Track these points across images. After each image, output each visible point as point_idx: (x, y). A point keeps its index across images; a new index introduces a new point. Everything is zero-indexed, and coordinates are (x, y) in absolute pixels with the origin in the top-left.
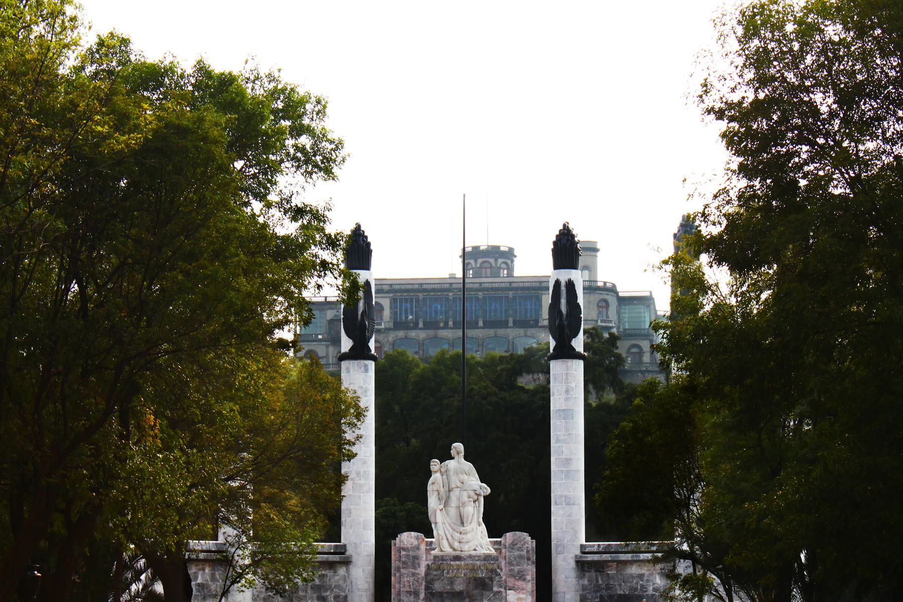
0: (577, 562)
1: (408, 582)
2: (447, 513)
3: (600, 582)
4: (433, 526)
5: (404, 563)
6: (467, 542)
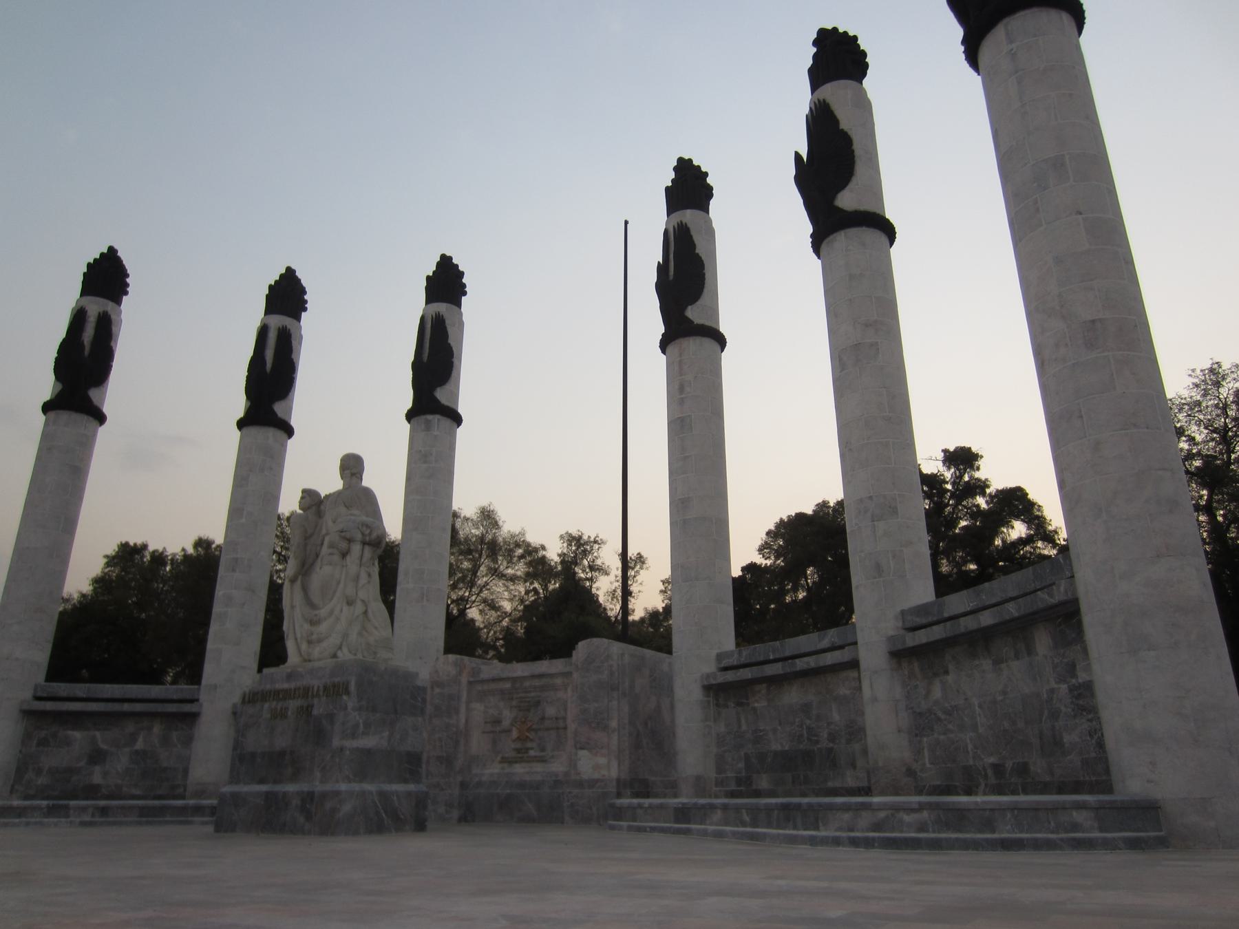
0: (708, 688)
2: (305, 589)
3: (744, 727)
6: (320, 641)
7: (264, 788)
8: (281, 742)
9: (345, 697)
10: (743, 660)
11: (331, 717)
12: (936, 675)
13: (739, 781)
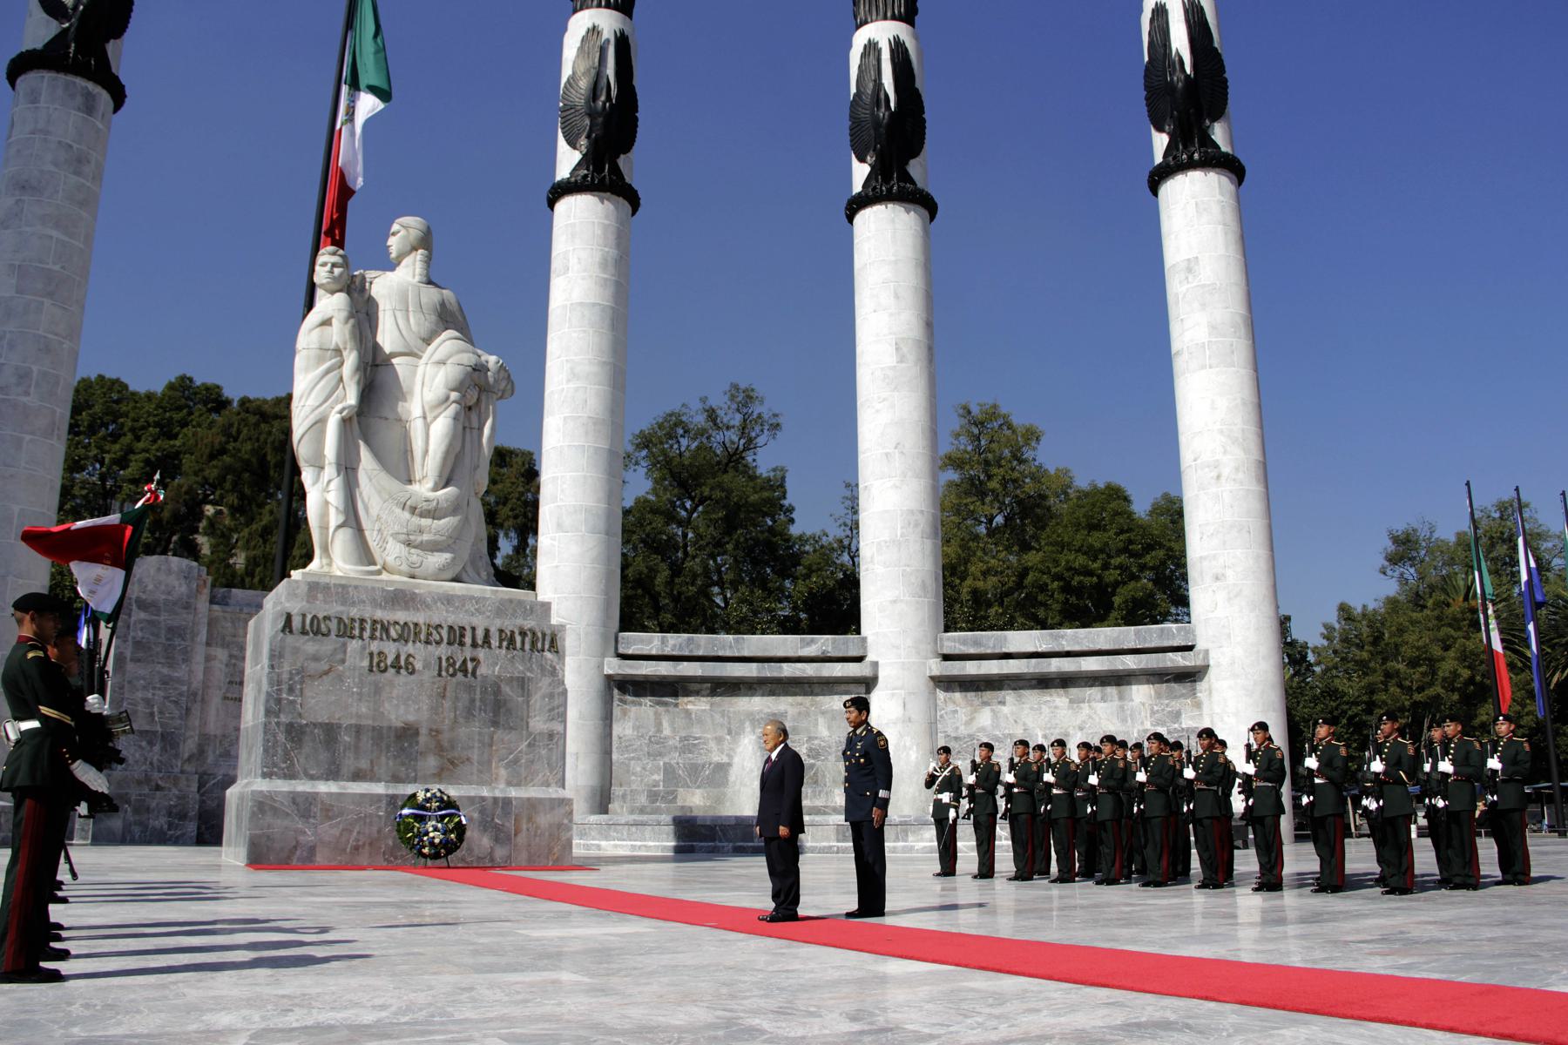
1: (148, 702)
3: (667, 731)
4: (307, 476)
5: (138, 644)
7: (379, 789)
8: (396, 713)
9: (548, 655)
10: (668, 651)
11: (522, 683)
12: (985, 704)
13: (653, 796)
